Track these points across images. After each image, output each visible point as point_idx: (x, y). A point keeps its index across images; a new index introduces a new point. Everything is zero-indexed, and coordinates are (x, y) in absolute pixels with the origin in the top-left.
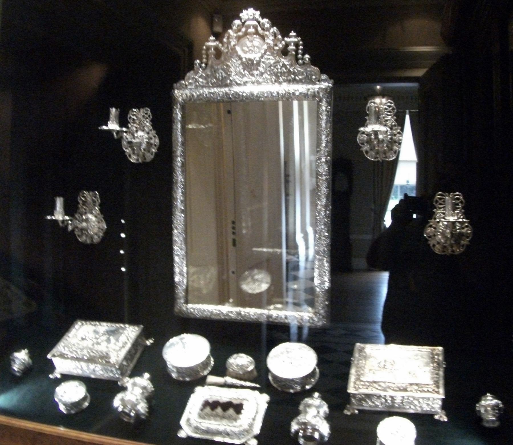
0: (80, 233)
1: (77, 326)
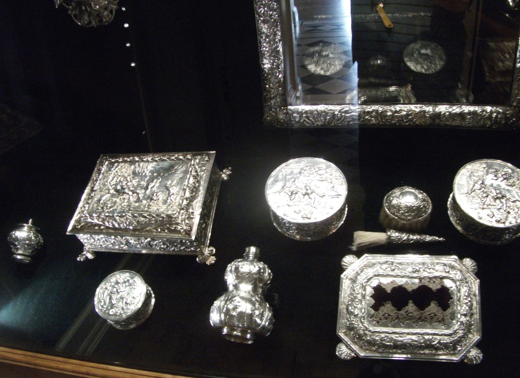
0: (77, 12)
1: (104, 169)
